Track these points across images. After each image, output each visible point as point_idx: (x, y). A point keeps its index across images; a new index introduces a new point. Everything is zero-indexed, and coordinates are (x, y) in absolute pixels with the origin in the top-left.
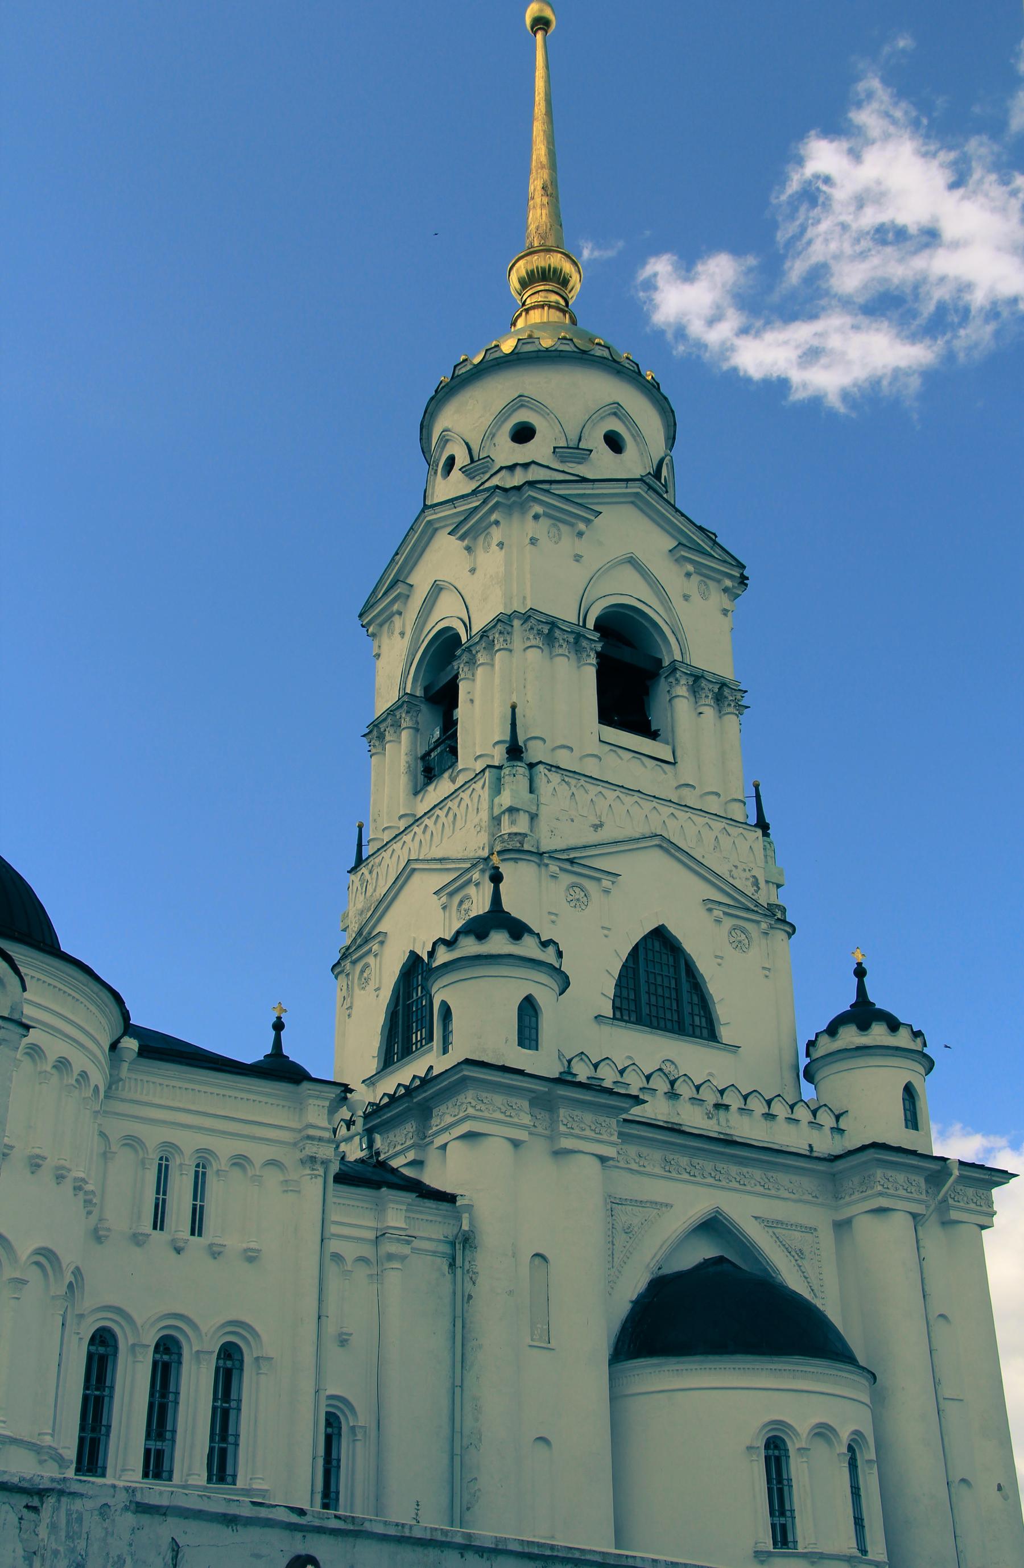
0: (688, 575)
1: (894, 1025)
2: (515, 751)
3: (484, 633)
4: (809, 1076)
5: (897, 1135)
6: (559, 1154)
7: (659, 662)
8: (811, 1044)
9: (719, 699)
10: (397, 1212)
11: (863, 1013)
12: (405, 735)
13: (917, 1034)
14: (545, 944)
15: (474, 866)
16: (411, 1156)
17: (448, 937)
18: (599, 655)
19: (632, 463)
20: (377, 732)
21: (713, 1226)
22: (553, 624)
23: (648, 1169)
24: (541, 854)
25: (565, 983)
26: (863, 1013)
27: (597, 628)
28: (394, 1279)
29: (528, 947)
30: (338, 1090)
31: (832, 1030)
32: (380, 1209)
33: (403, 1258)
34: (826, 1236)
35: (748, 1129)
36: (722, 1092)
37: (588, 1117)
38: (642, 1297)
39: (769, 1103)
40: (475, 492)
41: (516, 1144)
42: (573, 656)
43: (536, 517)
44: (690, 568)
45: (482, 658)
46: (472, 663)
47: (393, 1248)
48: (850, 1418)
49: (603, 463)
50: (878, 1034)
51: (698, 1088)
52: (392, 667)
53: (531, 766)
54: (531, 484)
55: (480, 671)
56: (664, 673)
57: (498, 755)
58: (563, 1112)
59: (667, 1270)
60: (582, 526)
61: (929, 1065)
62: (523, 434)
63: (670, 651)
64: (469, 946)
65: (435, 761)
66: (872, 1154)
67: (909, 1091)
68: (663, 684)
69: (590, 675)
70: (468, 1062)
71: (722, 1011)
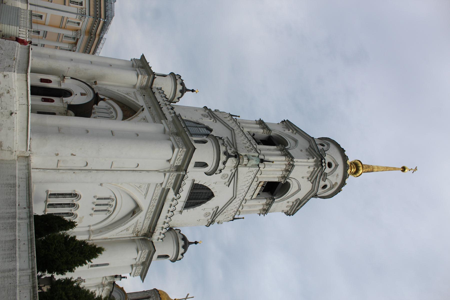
3: (289, 153)
7: (275, 195)
9: (264, 210)
15: (235, 149)
19: (320, 191)
22: (290, 172)
24: (237, 167)
27: (287, 182)
42: (281, 176)
44: (294, 203)
46: (281, 150)
53: (258, 165)
55: (279, 153)
60: (310, 179)
62: (330, 165)
63: (277, 198)
69: (276, 180)
71: (191, 210)
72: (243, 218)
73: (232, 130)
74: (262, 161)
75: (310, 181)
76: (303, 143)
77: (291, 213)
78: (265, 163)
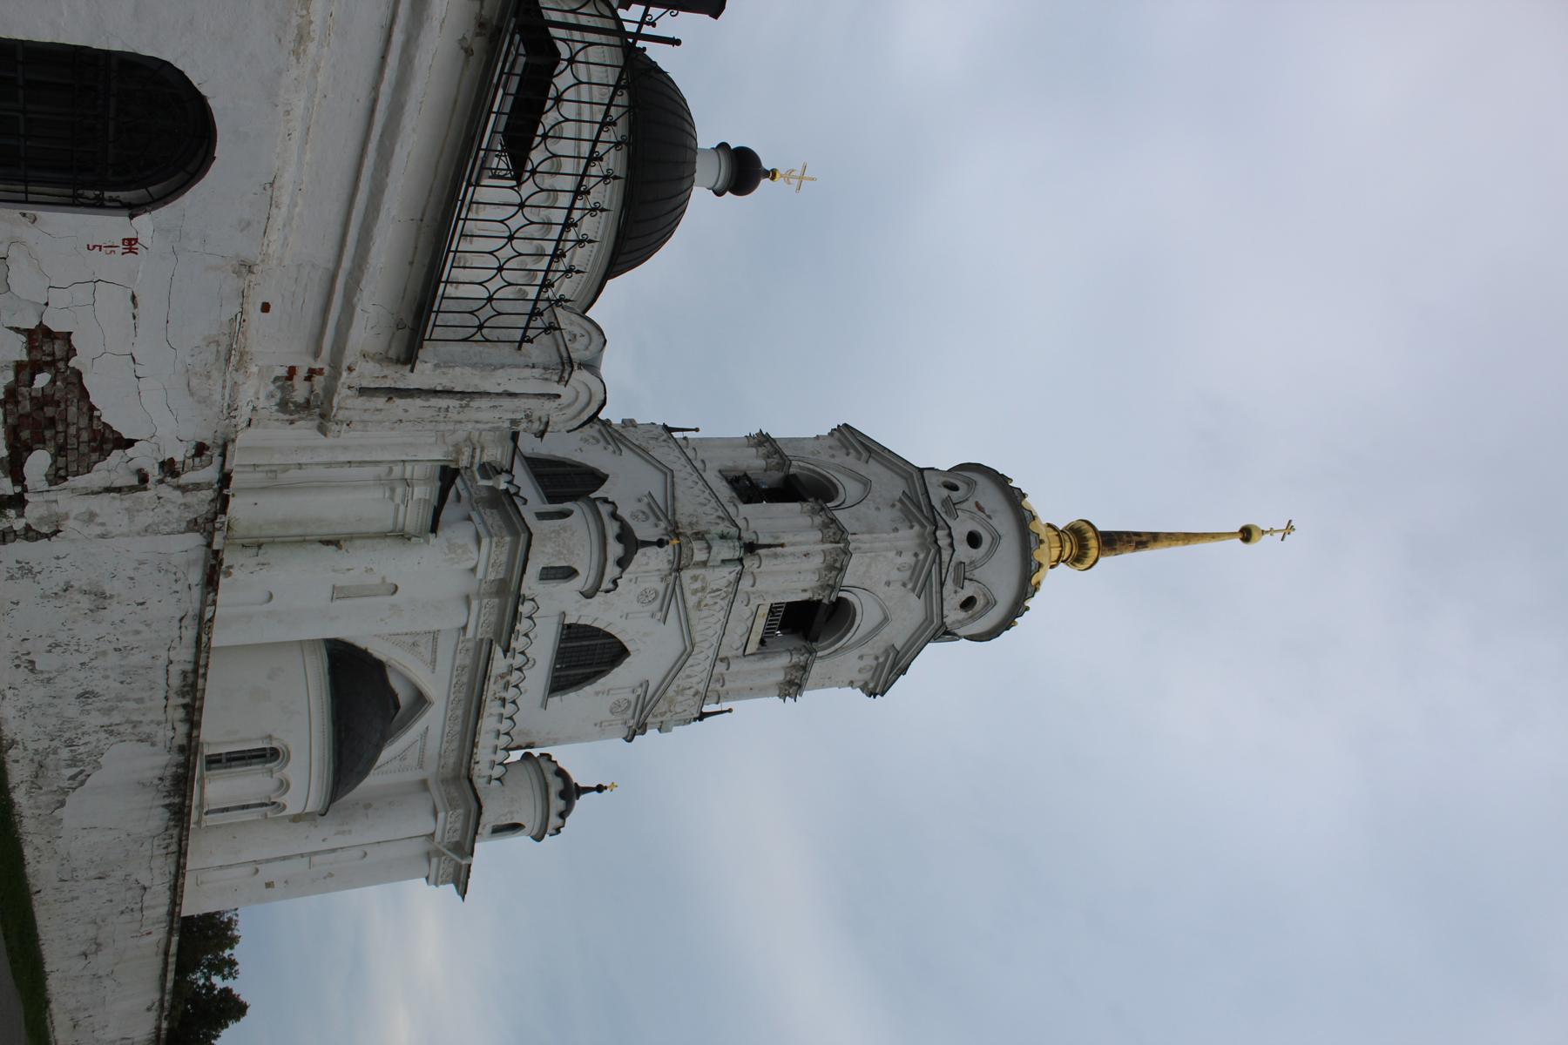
0: (877, 658)
1: (563, 815)
2: (751, 548)
3: (834, 521)
4: (527, 756)
5: (489, 818)
6: (467, 600)
7: (816, 640)
8: (548, 757)
9: (791, 683)
10: (424, 492)
11: (571, 792)
12: (762, 463)
13: (558, 831)
14: (615, 582)
16: (464, 494)
17: (619, 512)
18: (820, 601)
19: (953, 615)
21: (420, 700)
22: (842, 569)
23: (459, 656)
25: (588, 595)
26: (571, 792)
27: (839, 599)
28: (378, 494)
29: (612, 570)
30: (507, 467)
31: (561, 773)
32: (426, 480)
33: (392, 498)
34: (419, 775)
35: (488, 724)
36: (514, 702)
37: (493, 618)
38: (370, 656)
39: (507, 734)
40: (932, 508)
41: (473, 570)
43: (916, 555)
45: (818, 520)
46: (813, 512)
47: (399, 491)
48: (294, 803)
49: (953, 598)
50: (557, 804)
51: (516, 686)
53: (740, 560)
54: (939, 550)
56: (807, 644)
57: (748, 537)
58: (496, 601)
59: (388, 670)
60: (910, 586)
61: (538, 838)
62: (974, 540)
64: (612, 529)
66: (474, 806)
68: (800, 643)
70: (531, 534)
71: (572, 697)
72: (730, 711)
73: (668, 473)
74: (751, 548)
75: (913, 590)
76: (890, 486)
77: (876, 689)
78: (762, 552)
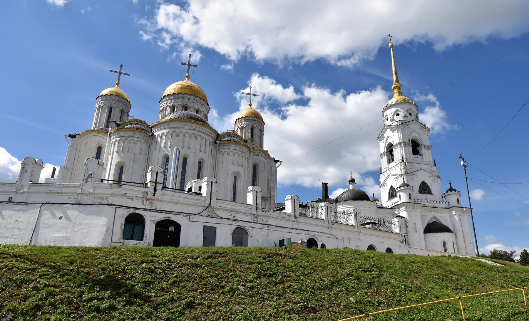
1: (455, 191)
9: (428, 148)
20: (381, 155)
26: (451, 189)
31: (447, 192)
34: (448, 218)
35: (437, 205)
45: (396, 147)
46: (395, 148)
50: (453, 191)
52: (382, 147)
57: (401, 161)
64: (402, 188)
65: (391, 159)
67: (458, 200)
69: (411, 148)
